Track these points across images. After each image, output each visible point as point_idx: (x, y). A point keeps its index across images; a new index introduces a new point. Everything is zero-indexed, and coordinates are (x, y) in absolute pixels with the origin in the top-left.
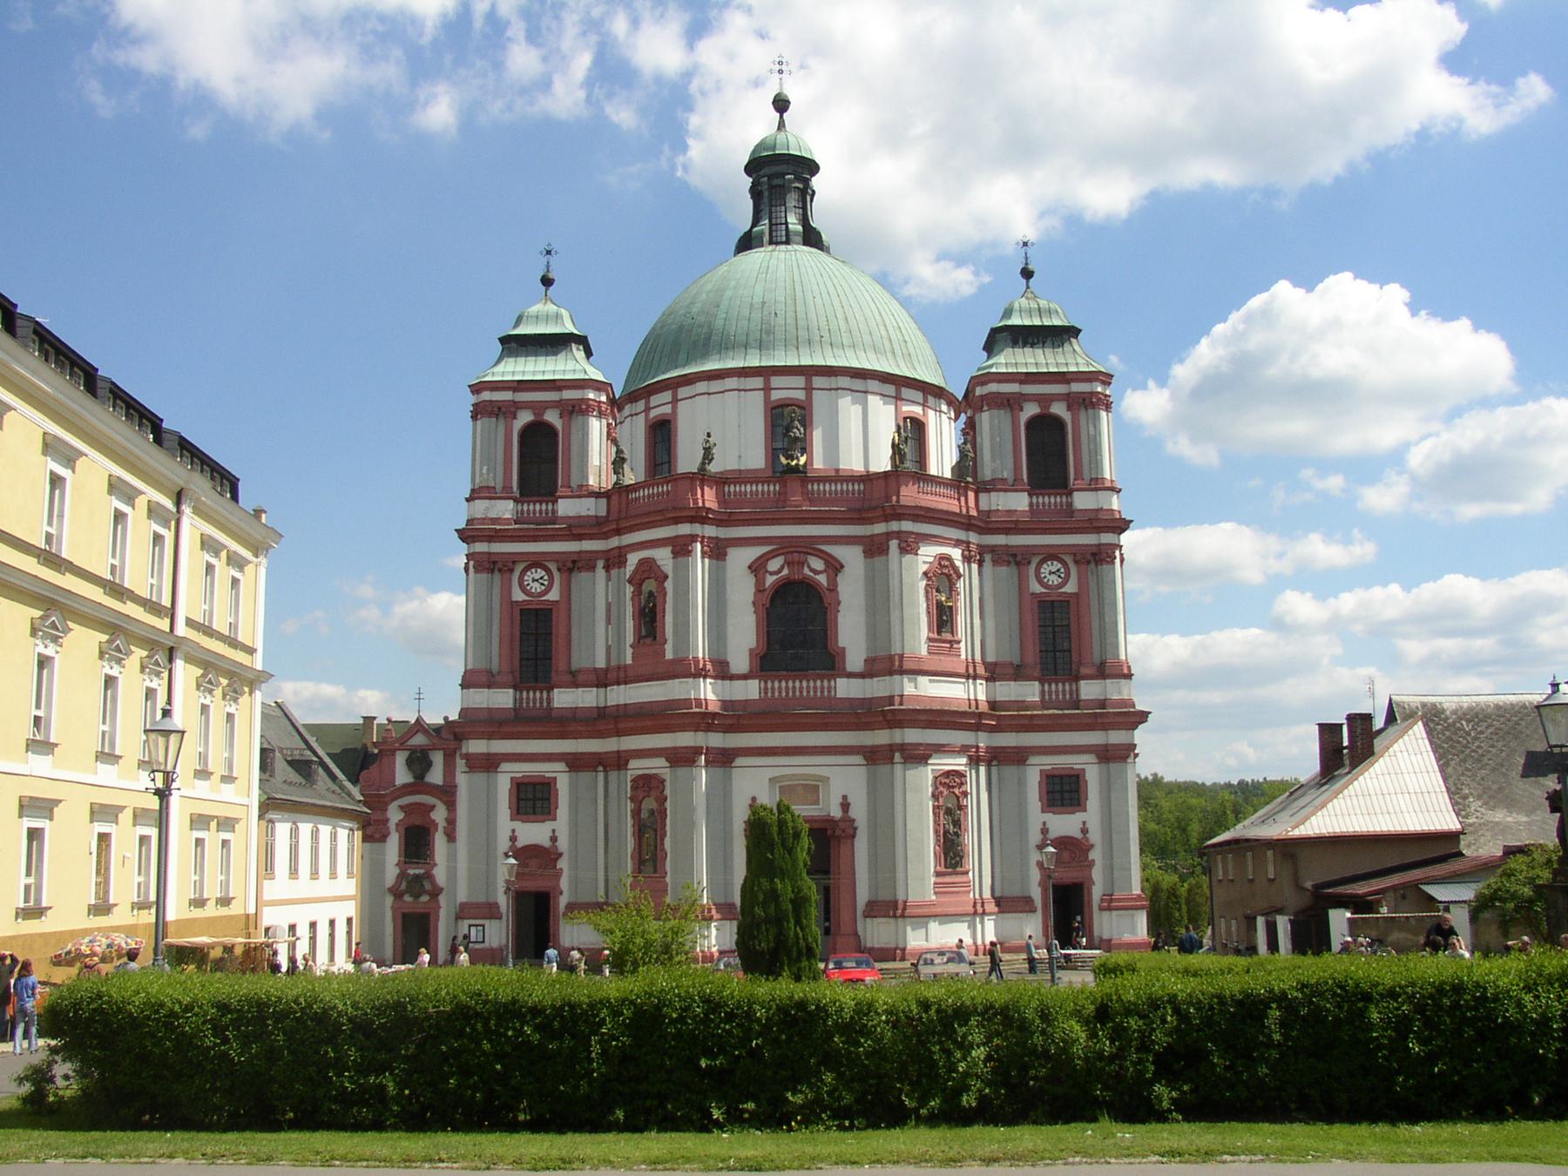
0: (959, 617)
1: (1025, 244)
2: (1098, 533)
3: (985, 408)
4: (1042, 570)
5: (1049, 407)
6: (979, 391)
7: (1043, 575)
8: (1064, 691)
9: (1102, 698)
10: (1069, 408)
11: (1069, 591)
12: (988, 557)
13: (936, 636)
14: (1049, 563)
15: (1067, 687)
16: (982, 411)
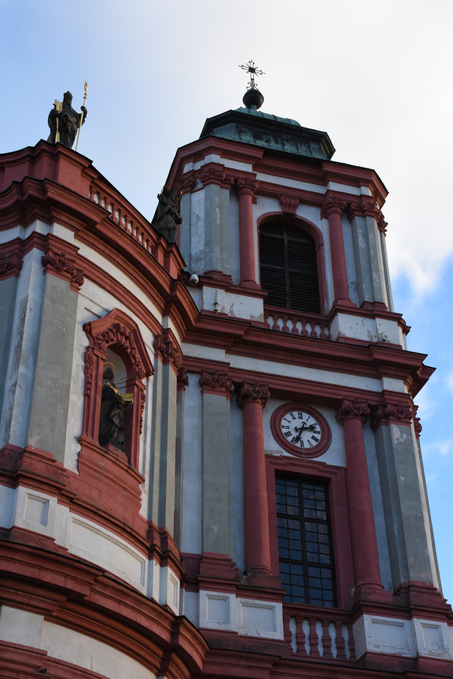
0: (142, 437)
1: (252, 70)
2: (379, 377)
3: (200, 186)
4: (284, 423)
5: (295, 207)
6: (187, 168)
7: (284, 431)
8: (326, 639)
9: (408, 654)
10: (324, 215)
11: (329, 463)
12: (193, 380)
13: (97, 443)
14: (296, 414)
15: (332, 633)
16: (192, 192)
